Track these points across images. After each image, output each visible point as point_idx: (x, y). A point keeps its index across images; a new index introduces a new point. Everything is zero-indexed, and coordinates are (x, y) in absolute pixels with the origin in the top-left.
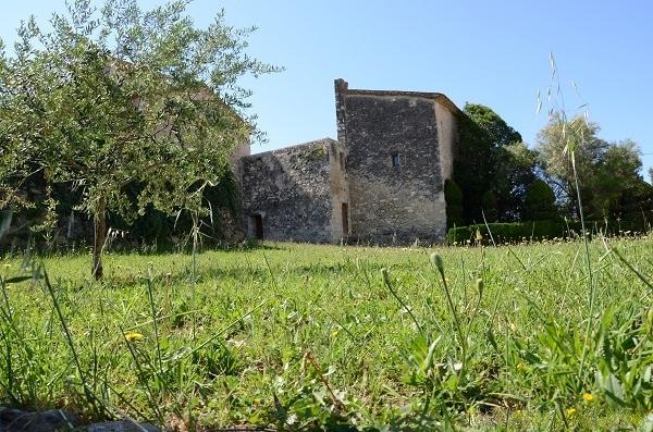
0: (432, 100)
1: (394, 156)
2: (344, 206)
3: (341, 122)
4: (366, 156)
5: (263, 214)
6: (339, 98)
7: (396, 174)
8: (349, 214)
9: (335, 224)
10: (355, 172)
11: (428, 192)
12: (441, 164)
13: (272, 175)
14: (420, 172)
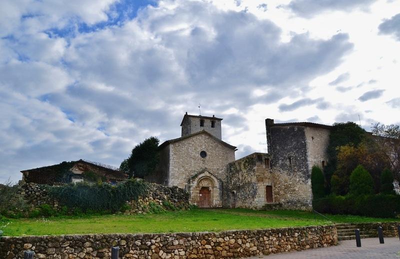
0: (303, 127)
1: (290, 159)
2: (269, 189)
5: (235, 192)
6: (267, 129)
7: (291, 170)
9: (260, 200)
10: (275, 168)
11: (304, 179)
12: (308, 162)
13: (238, 172)
14: (300, 167)
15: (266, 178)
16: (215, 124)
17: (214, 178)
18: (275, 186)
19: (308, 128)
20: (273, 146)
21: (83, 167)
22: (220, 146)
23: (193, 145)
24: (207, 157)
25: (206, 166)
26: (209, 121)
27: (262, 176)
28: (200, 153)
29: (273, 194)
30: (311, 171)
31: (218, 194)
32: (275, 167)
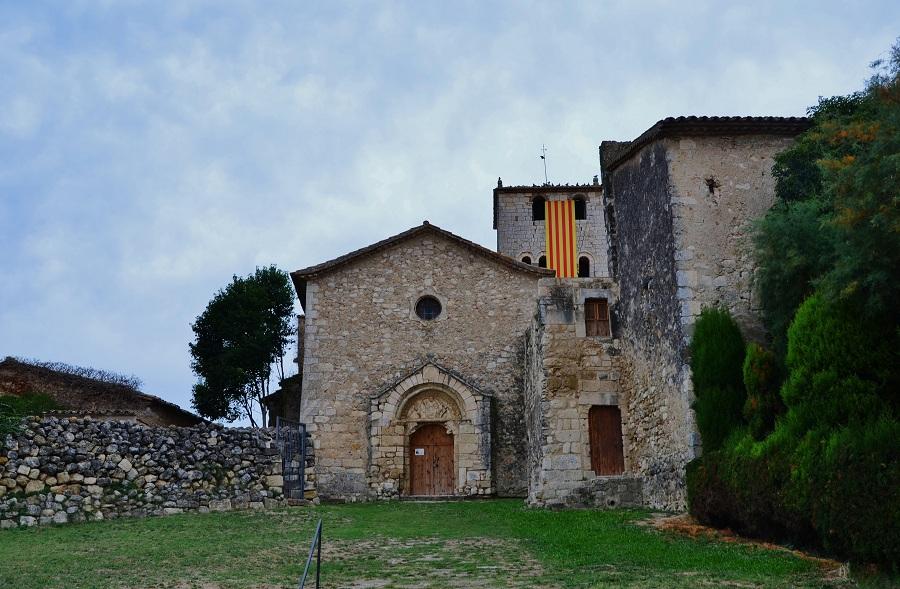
15: (592, 376)
16: (588, 206)
19: (687, 145)
21: (13, 380)
22: (491, 273)
23: (388, 278)
24: (442, 317)
25: (437, 350)
26: (564, 197)
27: (573, 368)
28: (413, 304)
30: (692, 333)
31: (475, 447)
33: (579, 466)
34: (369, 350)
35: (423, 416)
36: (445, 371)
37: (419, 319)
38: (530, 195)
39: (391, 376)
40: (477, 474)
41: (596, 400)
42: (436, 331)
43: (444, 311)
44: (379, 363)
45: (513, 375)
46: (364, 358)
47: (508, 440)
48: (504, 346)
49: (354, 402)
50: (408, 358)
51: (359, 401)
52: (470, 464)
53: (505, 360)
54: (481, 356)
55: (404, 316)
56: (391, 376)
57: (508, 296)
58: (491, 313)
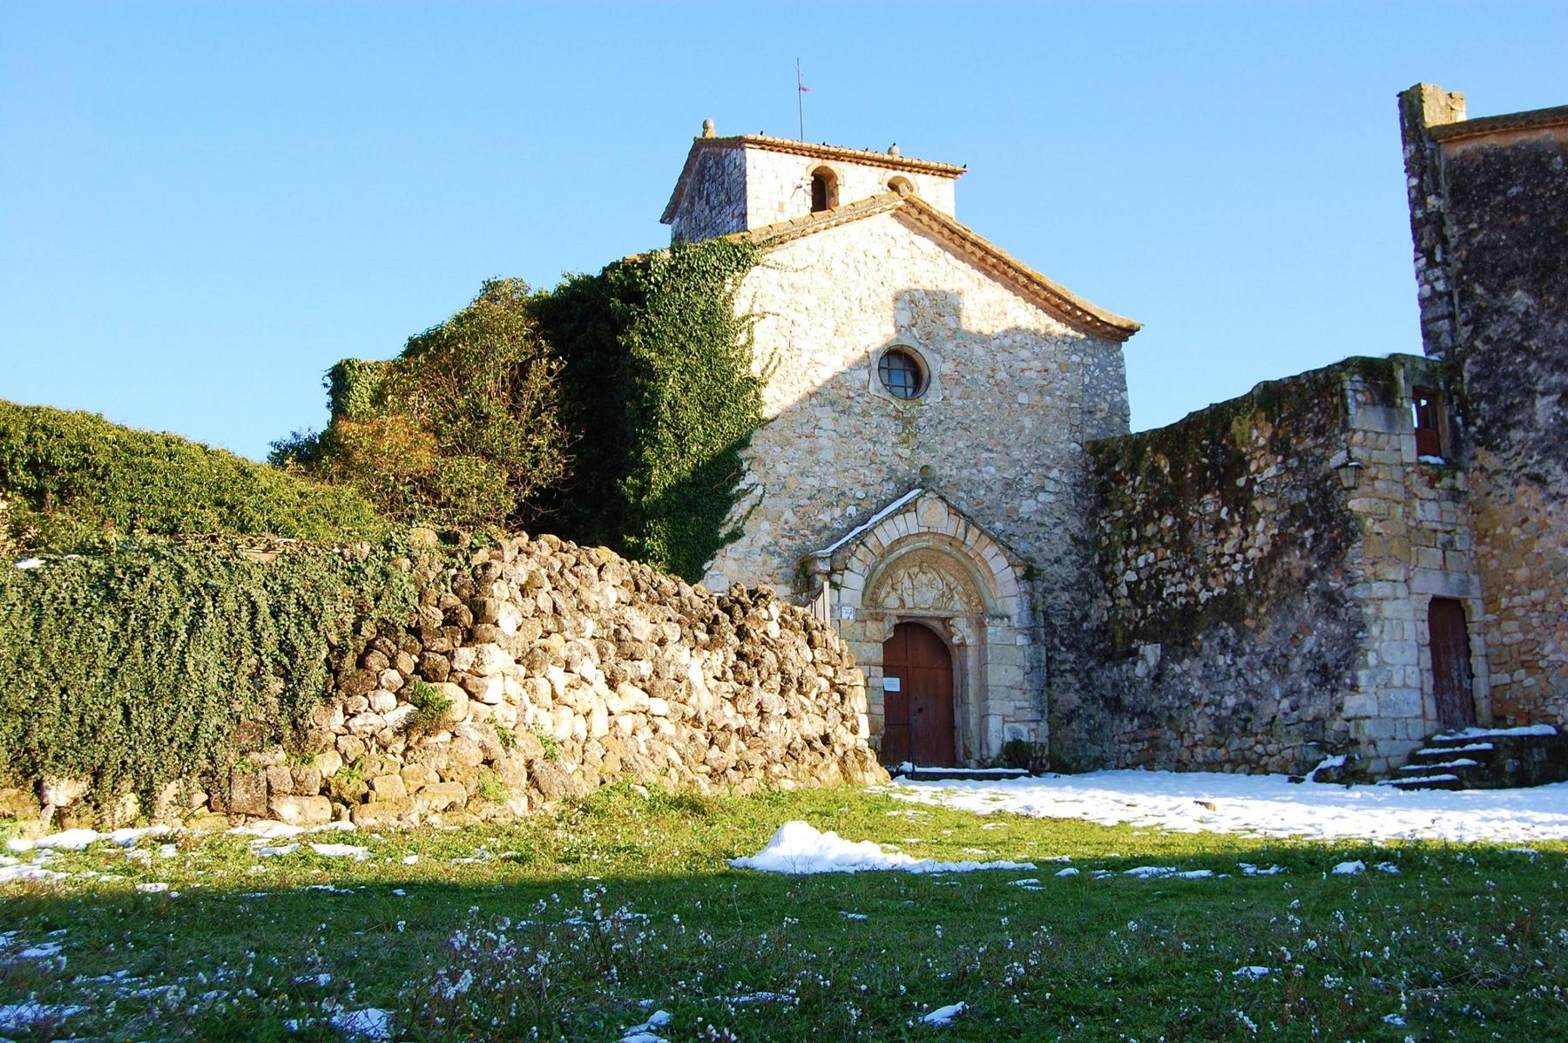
3: (1431, 263)
4: (1530, 394)
8: (1476, 643)
10: (1492, 461)
17: (990, 551)
18: (1490, 602)
20: (1466, 296)
24: (933, 397)
25: (924, 458)
29: (1478, 665)
31: (1016, 676)
32: (1492, 448)
33: (1419, 712)
34: (790, 452)
35: (909, 604)
36: (956, 511)
37: (887, 396)
38: (807, 160)
39: (837, 512)
40: (1023, 728)
41: (1436, 585)
42: (922, 422)
43: (936, 384)
44: (811, 481)
45: (1066, 529)
46: (781, 468)
47: (1063, 662)
48: (1049, 468)
49: (765, 563)
50: (870, 475)
51: (776, 561)
52: (1009, 707)
53: (1052, 498)
54: (1008, 484)
55: (857, 385)
56: (837, 512)
57: (1053, 366)
58: (1023, 398)
